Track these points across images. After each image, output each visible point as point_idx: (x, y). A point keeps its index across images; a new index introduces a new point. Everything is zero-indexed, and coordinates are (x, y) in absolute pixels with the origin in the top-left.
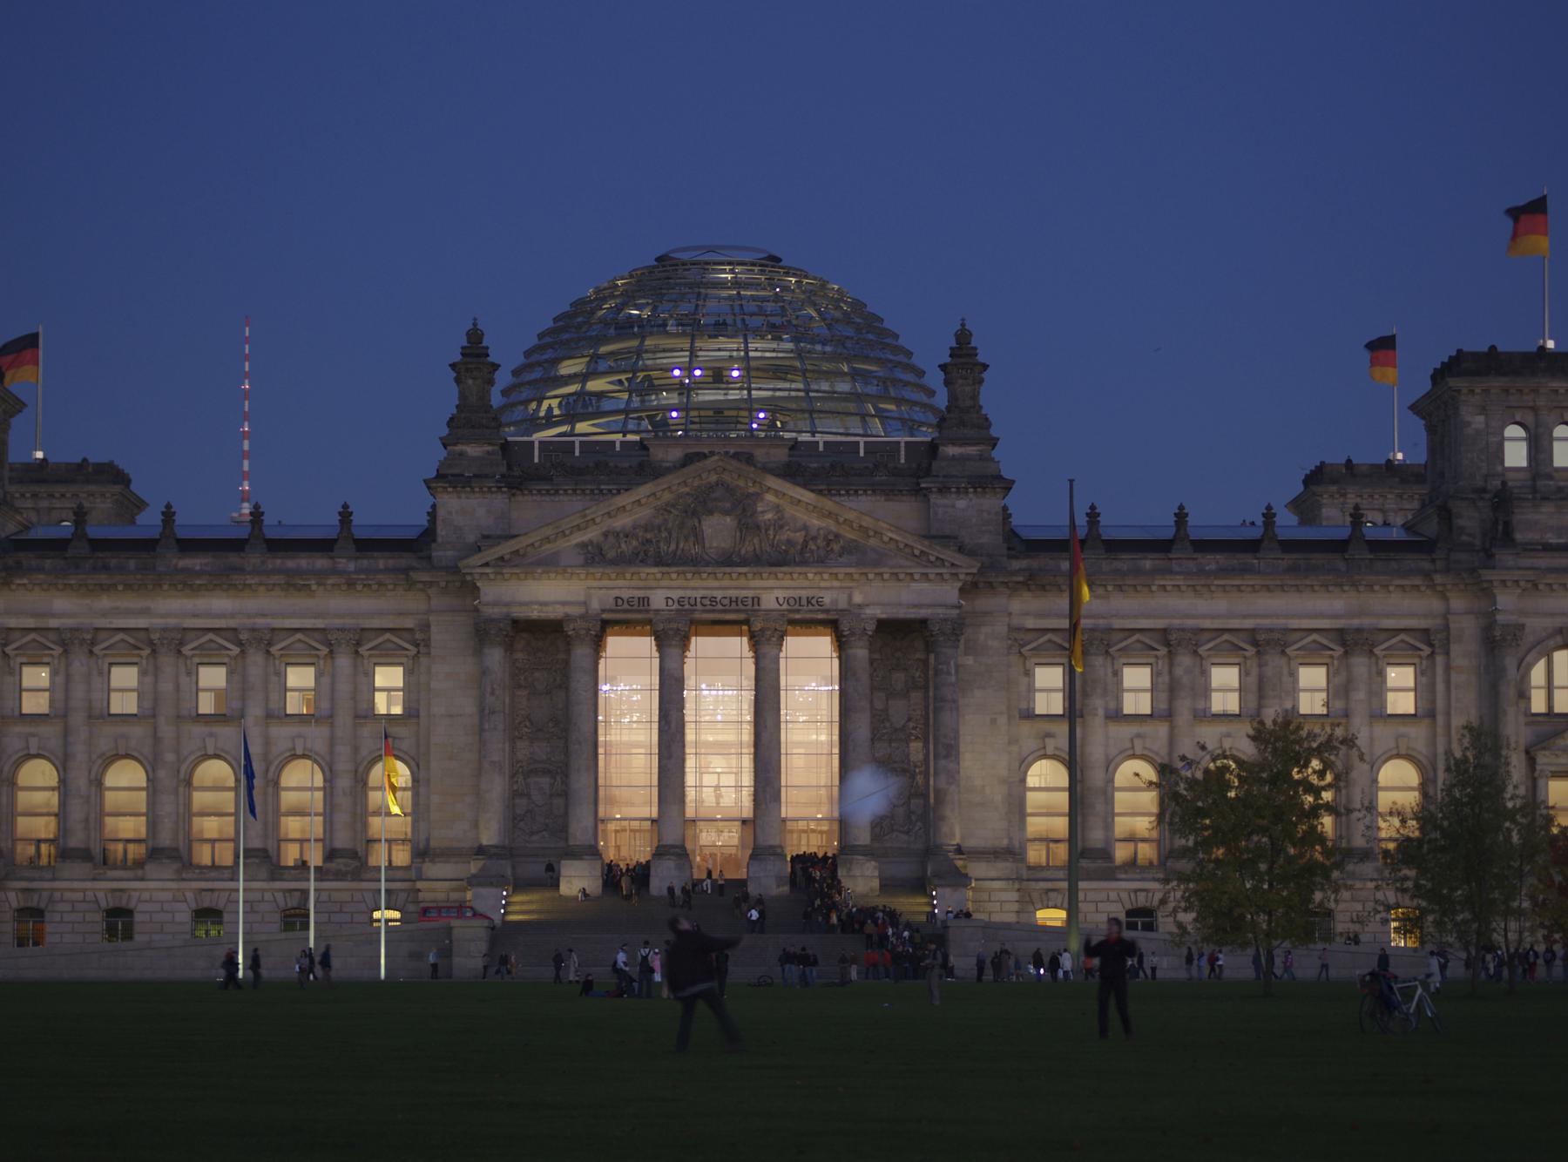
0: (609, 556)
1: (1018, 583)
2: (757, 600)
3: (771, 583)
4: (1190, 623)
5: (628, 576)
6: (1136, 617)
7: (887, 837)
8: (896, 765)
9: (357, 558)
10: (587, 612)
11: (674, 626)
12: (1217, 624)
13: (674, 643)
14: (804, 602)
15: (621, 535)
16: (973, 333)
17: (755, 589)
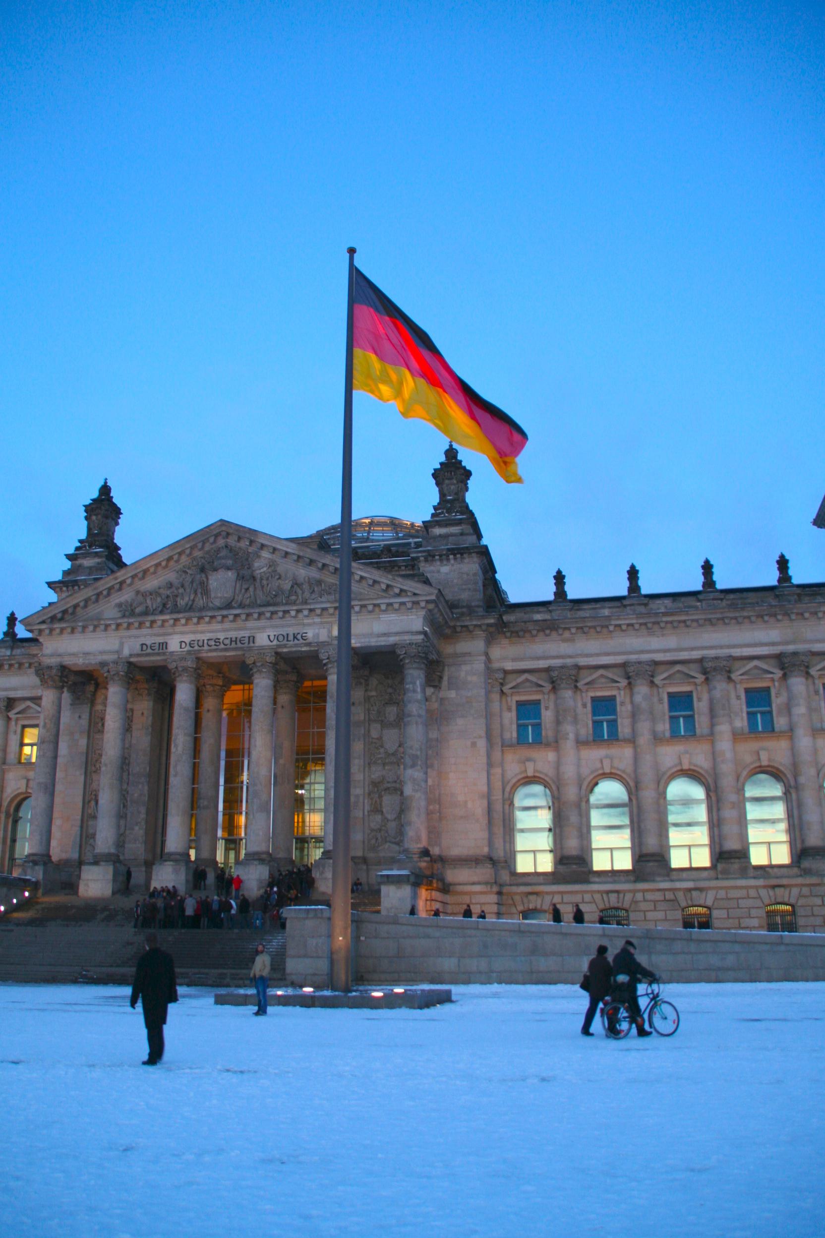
0: (138, 610)
1: (489, 625)
2: (252, 639)
3: (263, 622)
4: (645, 657)
5: (148, 624)
6: (598, 655)
7: (380, 848)
8: (389, 785)
9: (12, 648)
10: (119, 658)
11: (184, 664)
12: (668, 657)
13: (184, 678)
14: (291, 638)
15: (148, 594)
16: (459, 451)
17: (251, 629)
